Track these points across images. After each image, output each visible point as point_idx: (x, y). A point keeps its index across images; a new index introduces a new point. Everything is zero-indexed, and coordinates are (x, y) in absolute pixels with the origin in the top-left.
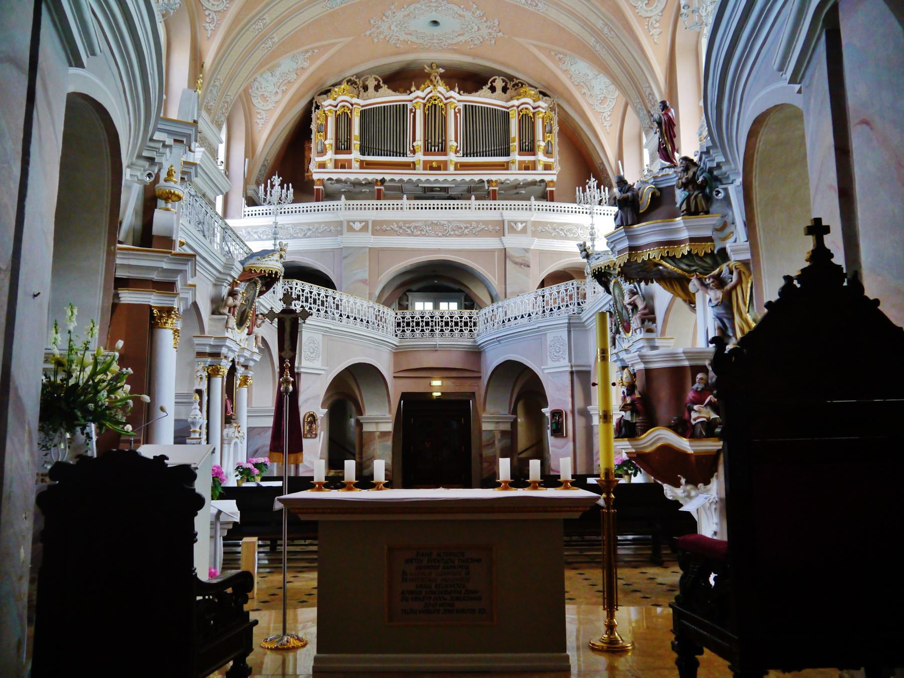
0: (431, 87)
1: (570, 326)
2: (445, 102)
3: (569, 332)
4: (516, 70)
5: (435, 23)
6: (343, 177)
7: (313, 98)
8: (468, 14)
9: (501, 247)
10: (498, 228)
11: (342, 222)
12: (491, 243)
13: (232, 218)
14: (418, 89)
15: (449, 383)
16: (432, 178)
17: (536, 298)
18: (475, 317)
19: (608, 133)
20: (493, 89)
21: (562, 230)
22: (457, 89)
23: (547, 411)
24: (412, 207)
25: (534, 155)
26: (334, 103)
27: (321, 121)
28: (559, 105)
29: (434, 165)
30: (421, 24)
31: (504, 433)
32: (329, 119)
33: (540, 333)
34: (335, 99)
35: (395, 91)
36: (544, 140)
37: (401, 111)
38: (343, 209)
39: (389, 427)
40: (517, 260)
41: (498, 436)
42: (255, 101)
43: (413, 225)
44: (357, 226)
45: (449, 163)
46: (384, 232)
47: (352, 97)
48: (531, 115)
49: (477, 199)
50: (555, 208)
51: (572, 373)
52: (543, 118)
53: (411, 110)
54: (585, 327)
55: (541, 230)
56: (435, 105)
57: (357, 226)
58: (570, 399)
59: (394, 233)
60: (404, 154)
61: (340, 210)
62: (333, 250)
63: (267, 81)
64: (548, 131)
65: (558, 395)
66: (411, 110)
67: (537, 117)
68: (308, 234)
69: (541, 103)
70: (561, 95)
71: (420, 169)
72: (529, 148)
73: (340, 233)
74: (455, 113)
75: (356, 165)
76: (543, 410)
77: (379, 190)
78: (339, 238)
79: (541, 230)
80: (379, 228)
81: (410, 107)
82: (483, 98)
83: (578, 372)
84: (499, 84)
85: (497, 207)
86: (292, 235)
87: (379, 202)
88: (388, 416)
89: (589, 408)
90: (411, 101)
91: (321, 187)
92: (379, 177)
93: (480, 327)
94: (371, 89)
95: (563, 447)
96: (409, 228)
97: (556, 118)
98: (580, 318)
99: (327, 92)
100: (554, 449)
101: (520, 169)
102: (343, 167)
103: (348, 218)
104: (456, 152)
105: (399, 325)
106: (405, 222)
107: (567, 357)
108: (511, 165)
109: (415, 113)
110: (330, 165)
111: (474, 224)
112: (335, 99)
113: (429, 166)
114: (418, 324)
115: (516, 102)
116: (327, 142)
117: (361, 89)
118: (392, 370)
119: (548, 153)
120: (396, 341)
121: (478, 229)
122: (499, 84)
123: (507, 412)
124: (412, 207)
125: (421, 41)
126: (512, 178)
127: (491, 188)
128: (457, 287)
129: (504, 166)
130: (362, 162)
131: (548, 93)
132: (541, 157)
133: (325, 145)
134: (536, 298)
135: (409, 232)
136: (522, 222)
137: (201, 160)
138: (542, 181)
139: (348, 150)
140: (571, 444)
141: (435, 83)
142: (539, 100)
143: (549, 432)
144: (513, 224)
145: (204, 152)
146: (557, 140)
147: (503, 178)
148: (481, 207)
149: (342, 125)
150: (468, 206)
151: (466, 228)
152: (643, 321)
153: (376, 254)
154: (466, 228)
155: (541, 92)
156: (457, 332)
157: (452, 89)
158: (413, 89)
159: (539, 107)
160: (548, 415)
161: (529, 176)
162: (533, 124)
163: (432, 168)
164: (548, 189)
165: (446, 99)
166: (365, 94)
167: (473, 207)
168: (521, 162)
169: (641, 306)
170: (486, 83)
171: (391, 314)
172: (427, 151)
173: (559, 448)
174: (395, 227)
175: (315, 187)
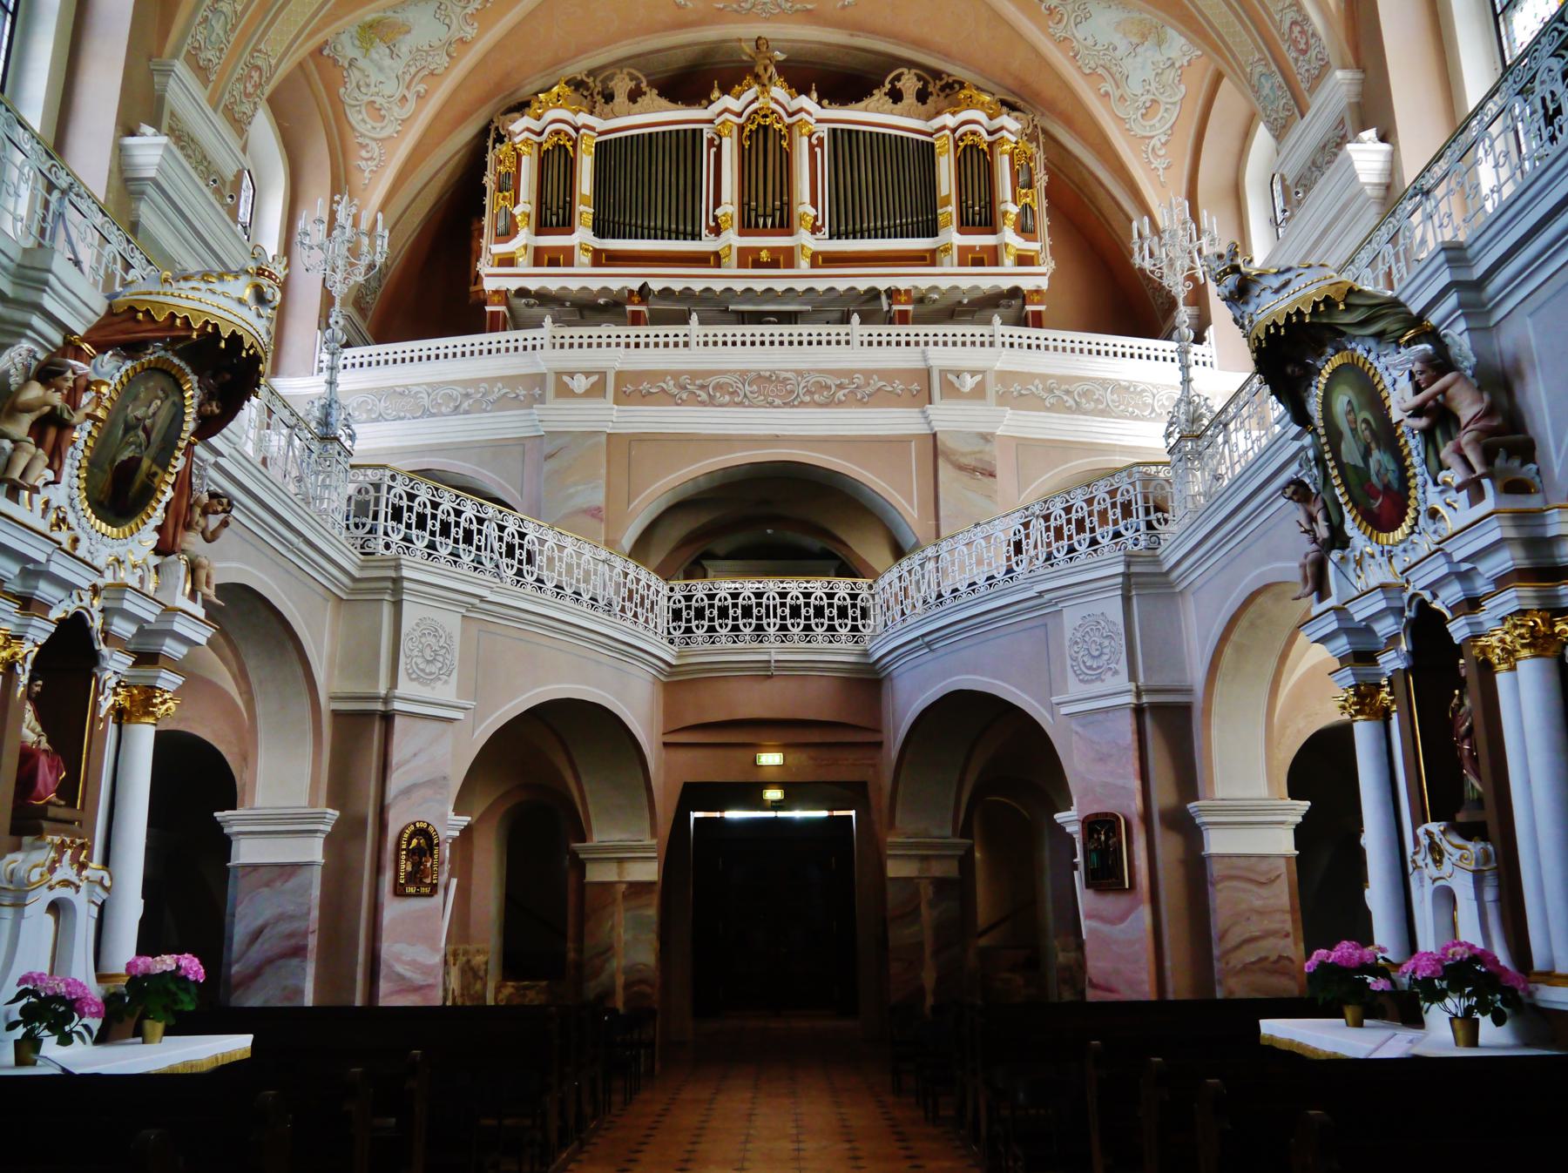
1: (1129, 584)
2: (788, 120)
3: (1127, 600)
4: (947, 56)
6: (553, 285)
9: (923, 429)
10: (915, 387)
11: (543, 376)
13: (291, 376)
15: (800, 758)
17: (1026, 525)
18: (864, 594)
19: (1163, 185)
20: (896, 96)
21: (1068, 392)
22: (815, 95)
23: (1070, 819)
24: (711, 339)
25: (994, 232)
28: (1045, 131)
29: (764, 255)
31: (940, 884)
32: (525, 159)
33: (1044, 608)
34: (539, 118)
37: (687, 144)
38: (547, 345)
39: (648, 872)
40: (964, 461)
41: (927, 892)
42: (354, 117)
43: (714, 380)
44: (580, 384)
45: (797, 252)
46: (645, 398)
47: (576, 112)
48: (985, 147)
51: (1139, 711)
53: (710, 141)
54: (1170, 585)
55: (1018, 391)
56: (766, 128)
57: (580, 384)
58: (1136, 784)
59: (667, 398)
60: (696, 236)
61: (545, 348)
63: (381, 69)
65: (1100, 773)
66: (711, 142)
68: (465, 405)
70: (1051, 108)
73: (541, 399)
74: (811, 147)
76: (1060, 817)
78: (537, 410)
79: (1018, 391)
80: (632, 389)
83: (1156, 708)
84: (909, 84)
88: (649, 841)
89: (1192, 806)
90: (711, 121)
91: (502, 309)
92: (635, 284)
93: (875, 620)
94: (621, 99)
95: (1122, 918)
96: (702, 387)
97: (1040, 157)
98: (1157, 561)
99: (521, 107)
100: (1094, 924)
101: (961, 264)
102: (554, 263)
103: (558, 366)
104: (815, 230)
105: (677, 614)
106: (694, 375)
107: (1123, 666)
109: (719, 147)
110: (524, 264)
112: (539, 118)
113: (749, 258)
114: (723, 613)
115: (948, 120)
116: (517, 211)
117: (598, 98)
118: (658, 728)
119: (1024, 230)
120: (668, 654)
121: (868, 390)
122: (909, 84)
123: (948, 831)
124: (711, 339)
127: (896, 308)
128: (815, 543)
129: (927, 258)
131: (1021, 103)
132: (1009, 237)
133: (513, 216)
134: (1026, 525)
135: (704, 396)
136: (973, 373)
137: (160, 169)
138: (1015, 292)
139: (566, 226)
140: (1145, 912)
143: (1079, 877)
144: (951, 377)
145: (166, 147)
146: (1045, 203)
147: (924, 284)
148: (875, 339)
149: (553, 173)
150: (843, 338)
151: (840, 387)
152: (1488, 456)
153: (623, 447)
155: (1004, 103)
156: (820, 630)
158: (716, 94)
159: (1001, 128)
160: (1074, 829)
161: (987, 281)
163: (757, 264)
164: (1029, 308)
165: (791, 115)
166: (608, 108)
167: (856, 340)
168: (963, 250)
169: (1467, 407)
170: (880, 84)
171: (662, 592)
172: (747, 227)
173: (1112, 921)
174: (670, 385)
175: (488, 309)
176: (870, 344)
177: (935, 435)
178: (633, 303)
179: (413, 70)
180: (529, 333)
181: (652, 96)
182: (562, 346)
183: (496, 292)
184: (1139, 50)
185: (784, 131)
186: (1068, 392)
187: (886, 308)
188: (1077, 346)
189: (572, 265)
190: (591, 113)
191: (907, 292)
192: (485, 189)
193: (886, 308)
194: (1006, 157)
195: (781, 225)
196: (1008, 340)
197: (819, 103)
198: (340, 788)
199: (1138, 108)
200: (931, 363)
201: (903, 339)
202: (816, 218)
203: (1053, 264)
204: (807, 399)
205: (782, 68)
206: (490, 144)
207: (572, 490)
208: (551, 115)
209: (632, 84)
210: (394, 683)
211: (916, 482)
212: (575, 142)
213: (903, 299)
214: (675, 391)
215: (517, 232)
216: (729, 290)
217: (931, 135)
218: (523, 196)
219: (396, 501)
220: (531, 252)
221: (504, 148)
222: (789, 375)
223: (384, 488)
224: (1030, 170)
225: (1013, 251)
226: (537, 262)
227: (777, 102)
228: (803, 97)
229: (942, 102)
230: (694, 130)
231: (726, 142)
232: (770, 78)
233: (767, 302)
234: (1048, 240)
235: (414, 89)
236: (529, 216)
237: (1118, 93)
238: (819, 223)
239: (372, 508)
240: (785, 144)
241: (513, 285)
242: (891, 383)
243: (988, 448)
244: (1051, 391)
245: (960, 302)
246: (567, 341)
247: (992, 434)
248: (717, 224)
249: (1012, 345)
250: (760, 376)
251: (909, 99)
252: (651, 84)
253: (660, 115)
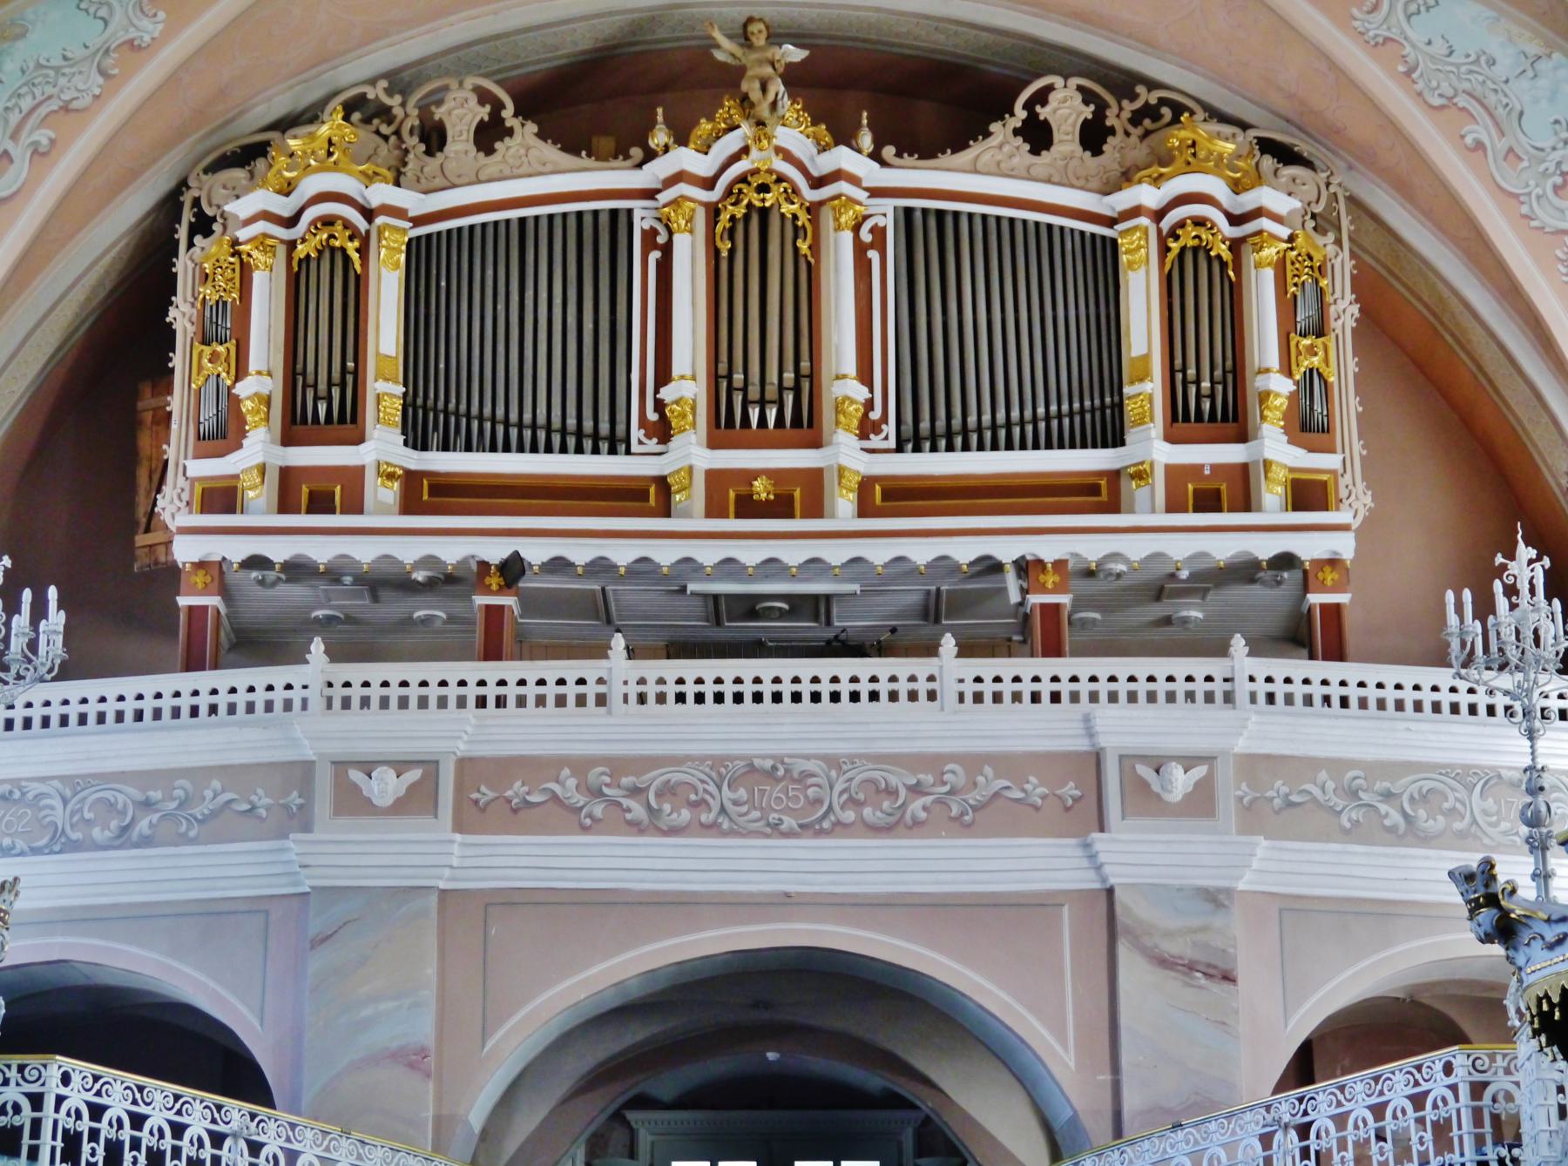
0: (746, 129)
2: (811, 195)
6: (321, 551)
7: (183, 184)
10: (1070, 790)
11: (307, 767)
12: (1038, 863)
14: (682, 141)
16: (751, 554)
17: (1266, 1140)
20: (1038, 136)
21: (1388, 796)
22: (866, 140)
24: (651, 690)
25: (1242, 437)
26: (284, 206)
27: (222, 288)
29: (761, 489)
32: (259, 278)
34: (287, 189)
35: (571, 148)
36: (1287, 371)
37: (602, 239)
38: (316, 703)
40: (1172, 948)
43: (657, 778)
45: (830, 481)
46: (517, 817)
47: (369, 178)
49: (967, 650)
50: (1353, 693)
52: (1280, 266)
53: (649, 235)
55: (1281, 798)
56: (764, 213)
57: (385, 787)
59: (567, 817)
60: (617, 443)
61: (306, 709)
62: (259, 906)
64: (1304, 322)
66: (649, 235)
67: (1250, 258)
68: (143, 826)
69: (1266, 197)
70: (1366, 159)
71: (691, 512)
72: (1214, 403)
73: (302, 820)
74: (860, 249)
75: (382, 494)
77: (494, 613)
78: (295, 845)
79: (1281, 798)
80: (489, 795)
82: (985, 176)
84: (1066, 110)
85: (1065, 688)
86: (57, 833)
87: (491, 671)
90: (650, 194)
91: (213, 601)
92: (495, 551)
94: (460, 142)
96: (635, 792)
97: (1343, 266)
99: (248, 155)
101: (1173, 507)
102: (321, 503)
103: (339, 749)
104: (867, 429)
106: (618, 765)
108: (1128, 486)
109: (667, 250)
110: (259, 499)
111: (956, 775)
112: (287, 189)
115: (1147, 195)
116: (244, 389)
117: (412, 141)
119: (1308, 426)
121: (974, 797)
122: (1066, 110)
124: (651, 690)
126: (1137, 548)
127: (1035, 599)
128: (874, 1080)
129: (1100, 494)
130: (411, 479)
131: (1303, 147)
132: (1275, 447)
133: (235, 401)
135: (637, 811)
136: (1189, 762)
138: (1286, 561)
139: (347, 423)
141: (763, 111)
142: (1258, 180)
144: (1145, 771)
146: (1352, 365)
147: (1091, 549)
148: (988, 688)
150: (922, 687)
151: (916, 790)
153: (474, 919)
154: (916, 790)
155: (1267, 146)
157: (844, 136)
158: (659, 138)
163: (749, 507)
164: (1315, 599)
165: (818, 183)
166: (433, 164)
167: (949, 690)
168: (1176, 474)
172: (726, 426)
174: (568, 788)
175: (183, 601)
176: (978, 698)
177: (1110, 892)
178: (488, 591)
179: (26, 104)
180: (278, 675)
181: (524, 137)
182: (346, 702)
183: (201, 565)
184: (1542, 65)
185: (803, 219)
186: (1388, 796)
187: (1014, 597)
188: (1409, 696)
189: (359, 510)
190: (397, 184)
191: (1059, 565)
192: (174, 332)
193: (1014, 597)
194: (1269, 274)
195: (797, 422)
196: (1262, 688)
197: (876, 156)
199: (1545, 174)
200: (1103, 741)
201: (1046, 688)
202: (869, 405)
203: (1368, 500)
204: (849, 816)
205: (795, 78)
206: (182, 234)
207: (366, 1012)
208: (312, 185)
209: (484, 112)
211: (1072, 989)
212: (365, 240)
213: (1050, 579)
214: (579, 799)
215: (243, 434)
216: (688, 560)
217: (1111, 222)
218: (255, 361)
219: (70, 1123)
220: (273, 478)
221: (210, 249)
222: (811, 766)
223: (50, 1102)
224: (1321, 293)
225: (1280, 474)
226: (286, 505)
227: (788, 156)
228: (843, 150)
230: (614, 213)
231: (682, 244)
232: (774, 105)
233: (767, 577)
234: (1357, 446)
235: (25, 138)
236: (268, 402)
237: (1502, 145)
238: (875, 415)
239: (26, 1141)
240: (804, 247)
241: (236, 550)
242: (1021, 782)
243: (1218, 921)
244: (1354, 794)
245: (1172, 576)
246: (356, 692)
247: (1229, 892)
248: (663, 416)
249: (1271, 698)
250: (752, 769)
252: (521, 112)
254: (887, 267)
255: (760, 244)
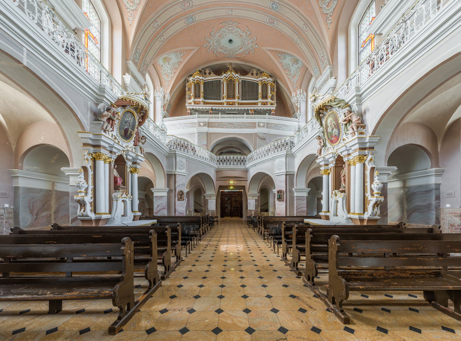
5: (230, 41)
8: (244, 34)
20: (252, 74)
23: (275, 191)
30: (224, 42)
37: (218, 83)
43: (223, 124)
46: (213, 127)
51: (286, 175)
58: (285, 186)
60: (220, 100)
64: (272, 90)
65: (280, 184)
72: (265, 97)
74: (239, 84)
81: (222, 80)
82: (248, 78)
83: (289, 174)
84: (255, 72)
94: (207, 74)
97: (275, 86)
99: (191, 75)
103: (199, 121)
104: (239, 99)
106: (220, 123)
110: (193, 103)
111: (246, 124)
115: (260, 79)
116: (192, 94)
119: (272, 99)
122: (255, 72)
125: (225, 53)
132: (269, 100)
143: (276, 199)
147: (256, 108)
155: (270, 76)
162: (267, 87)
163: (230, 104)
174: (216, 125)
198: (168, 185)
208: (196, 77)
210: (176, 170)
221: (188, 83)
226: (195, 104)
229: (260, 75)
241: (191, 108)
251: (255, 75)
253: (213, 77)
254: (241, 85)
255: (231, 82)
